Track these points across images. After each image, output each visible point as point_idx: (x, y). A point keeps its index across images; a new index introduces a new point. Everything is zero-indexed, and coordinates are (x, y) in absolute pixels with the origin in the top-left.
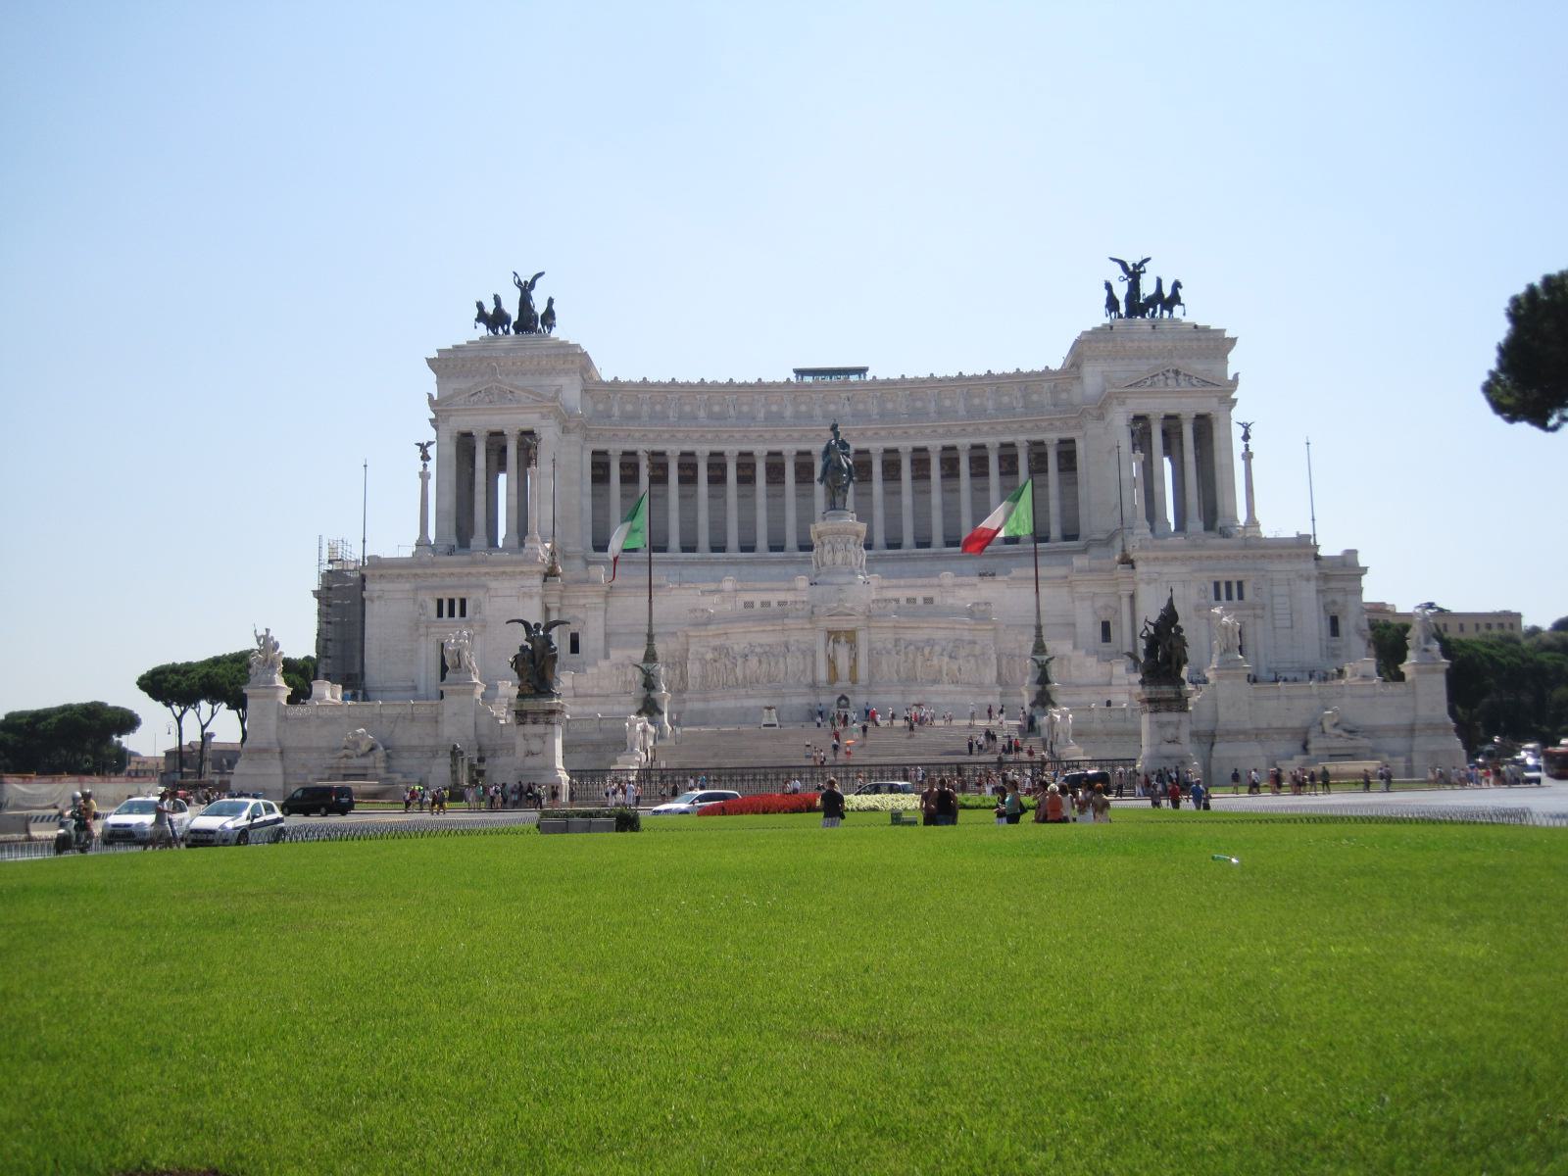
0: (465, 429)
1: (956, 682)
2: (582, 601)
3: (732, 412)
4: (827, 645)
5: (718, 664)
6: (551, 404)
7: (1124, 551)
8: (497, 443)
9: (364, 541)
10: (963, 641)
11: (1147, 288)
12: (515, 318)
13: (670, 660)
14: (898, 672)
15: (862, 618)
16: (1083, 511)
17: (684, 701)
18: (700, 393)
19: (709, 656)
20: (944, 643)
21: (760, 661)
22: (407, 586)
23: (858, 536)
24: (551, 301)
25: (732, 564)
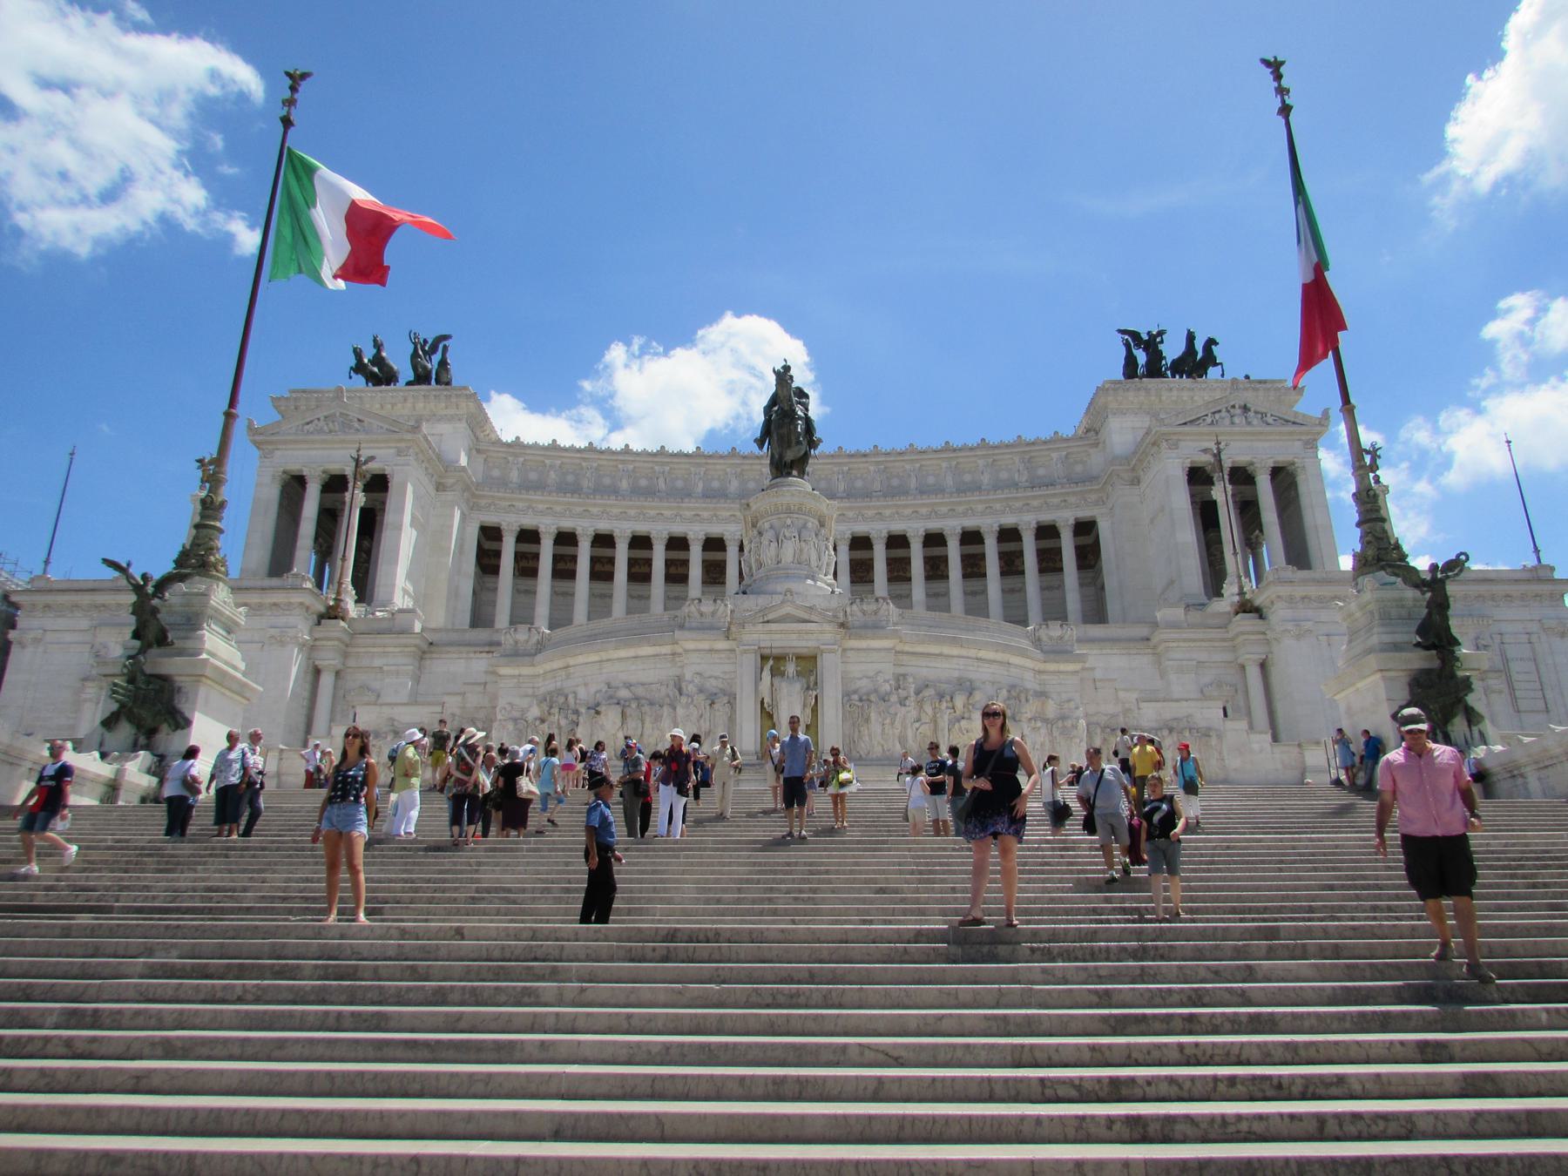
0: (294, 467)
2: (377, 662)
3: (662, 485)
6: (409, 436)
7: (1241, 593)
8: (335, 484)
9: (47, 562)
10: (1027, 690)
11: (1172, 349)
12: (405, 372)
14: (902, 740)
15: (827, 627)
16: (1112, 607)
18: (623, 462)
19: (535, 712)
21: (623, 714)
22: (84, 623)
23: (822, 525)
24: (445, 348)
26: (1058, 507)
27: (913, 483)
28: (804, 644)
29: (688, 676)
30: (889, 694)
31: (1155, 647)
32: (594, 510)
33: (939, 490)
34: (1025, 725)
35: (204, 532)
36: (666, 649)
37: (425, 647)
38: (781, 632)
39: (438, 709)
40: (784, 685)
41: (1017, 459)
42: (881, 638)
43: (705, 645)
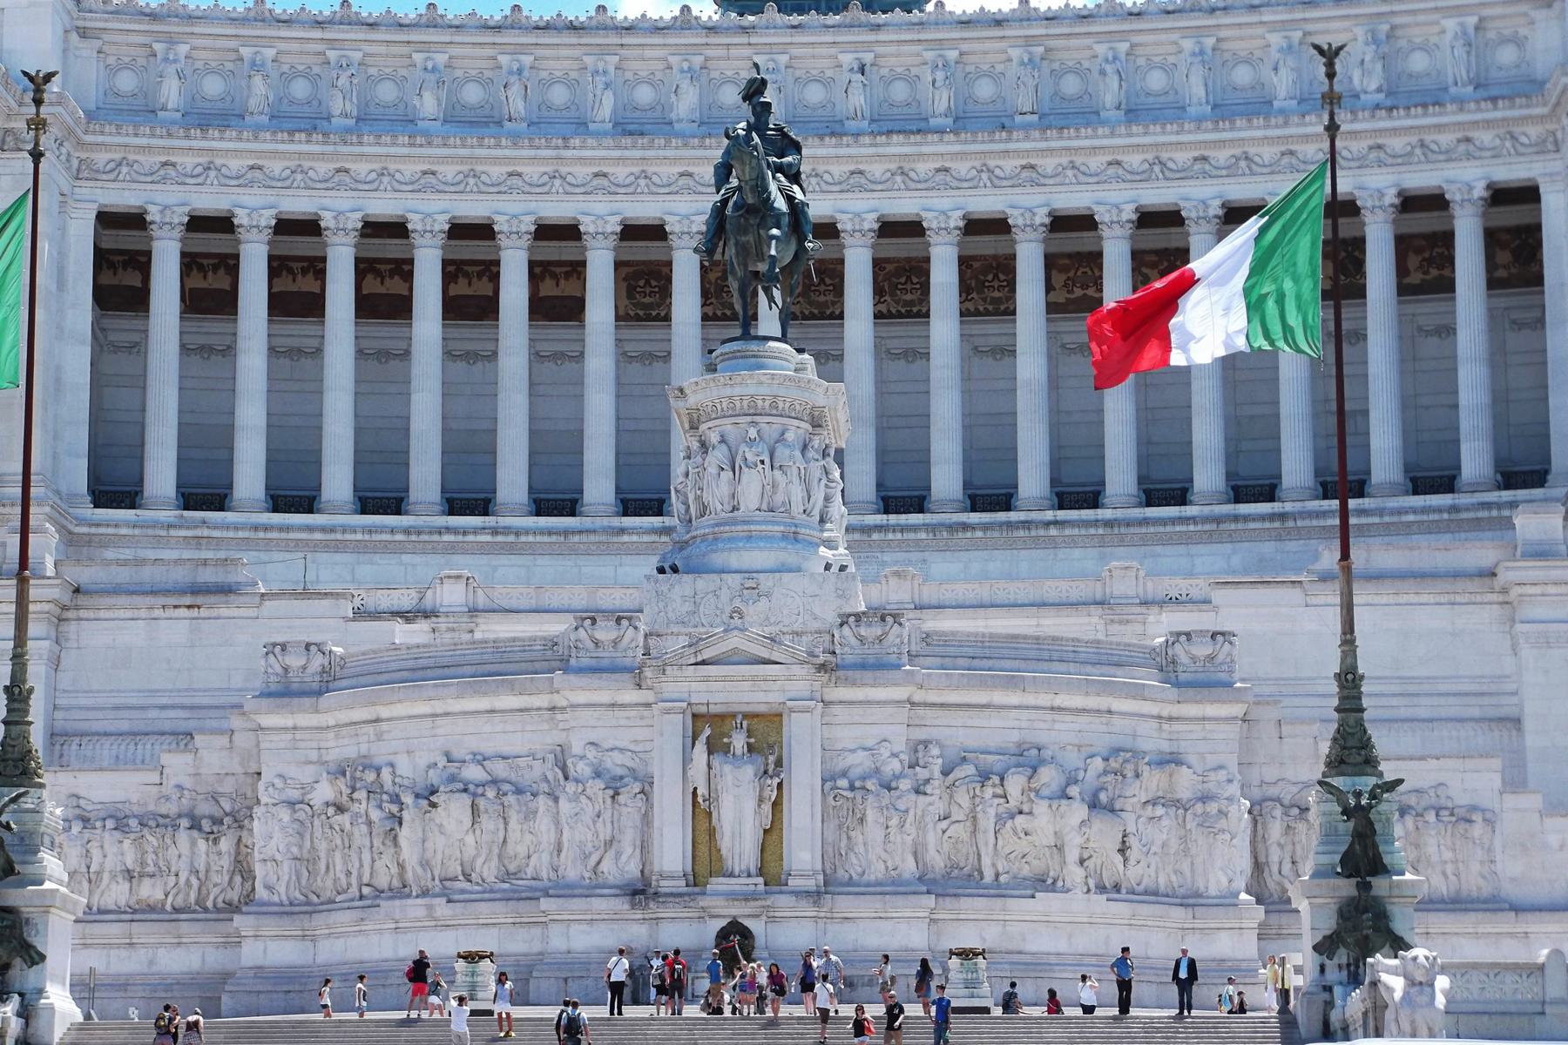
1: (1112, 889)
3: (517, 105)
4: (686, 761)
5: (345, 819)
10: (1137, 754)
13: (205, 808)
15: (797, 670)
17: (234, 942)
18: (424, 47)
20: (1072, 759)
23: (816, 423)
25: (510, 549)
26: (1449, 155)
27: (1110, 93)
28: (761, 697)
29: (577, 748)
30: (897, 777)
31: (1505, 591)
32: (361, 169)
33: (1169, 110)
34: (1129, 818)
35: (15, 730)
36: (542, 701)
37: (66, 598)
38: (725, 679)
39: (155, 778)
40: (727, 768)
41: (1360, 32)
42: (885, 685)
43: (604, 697)
